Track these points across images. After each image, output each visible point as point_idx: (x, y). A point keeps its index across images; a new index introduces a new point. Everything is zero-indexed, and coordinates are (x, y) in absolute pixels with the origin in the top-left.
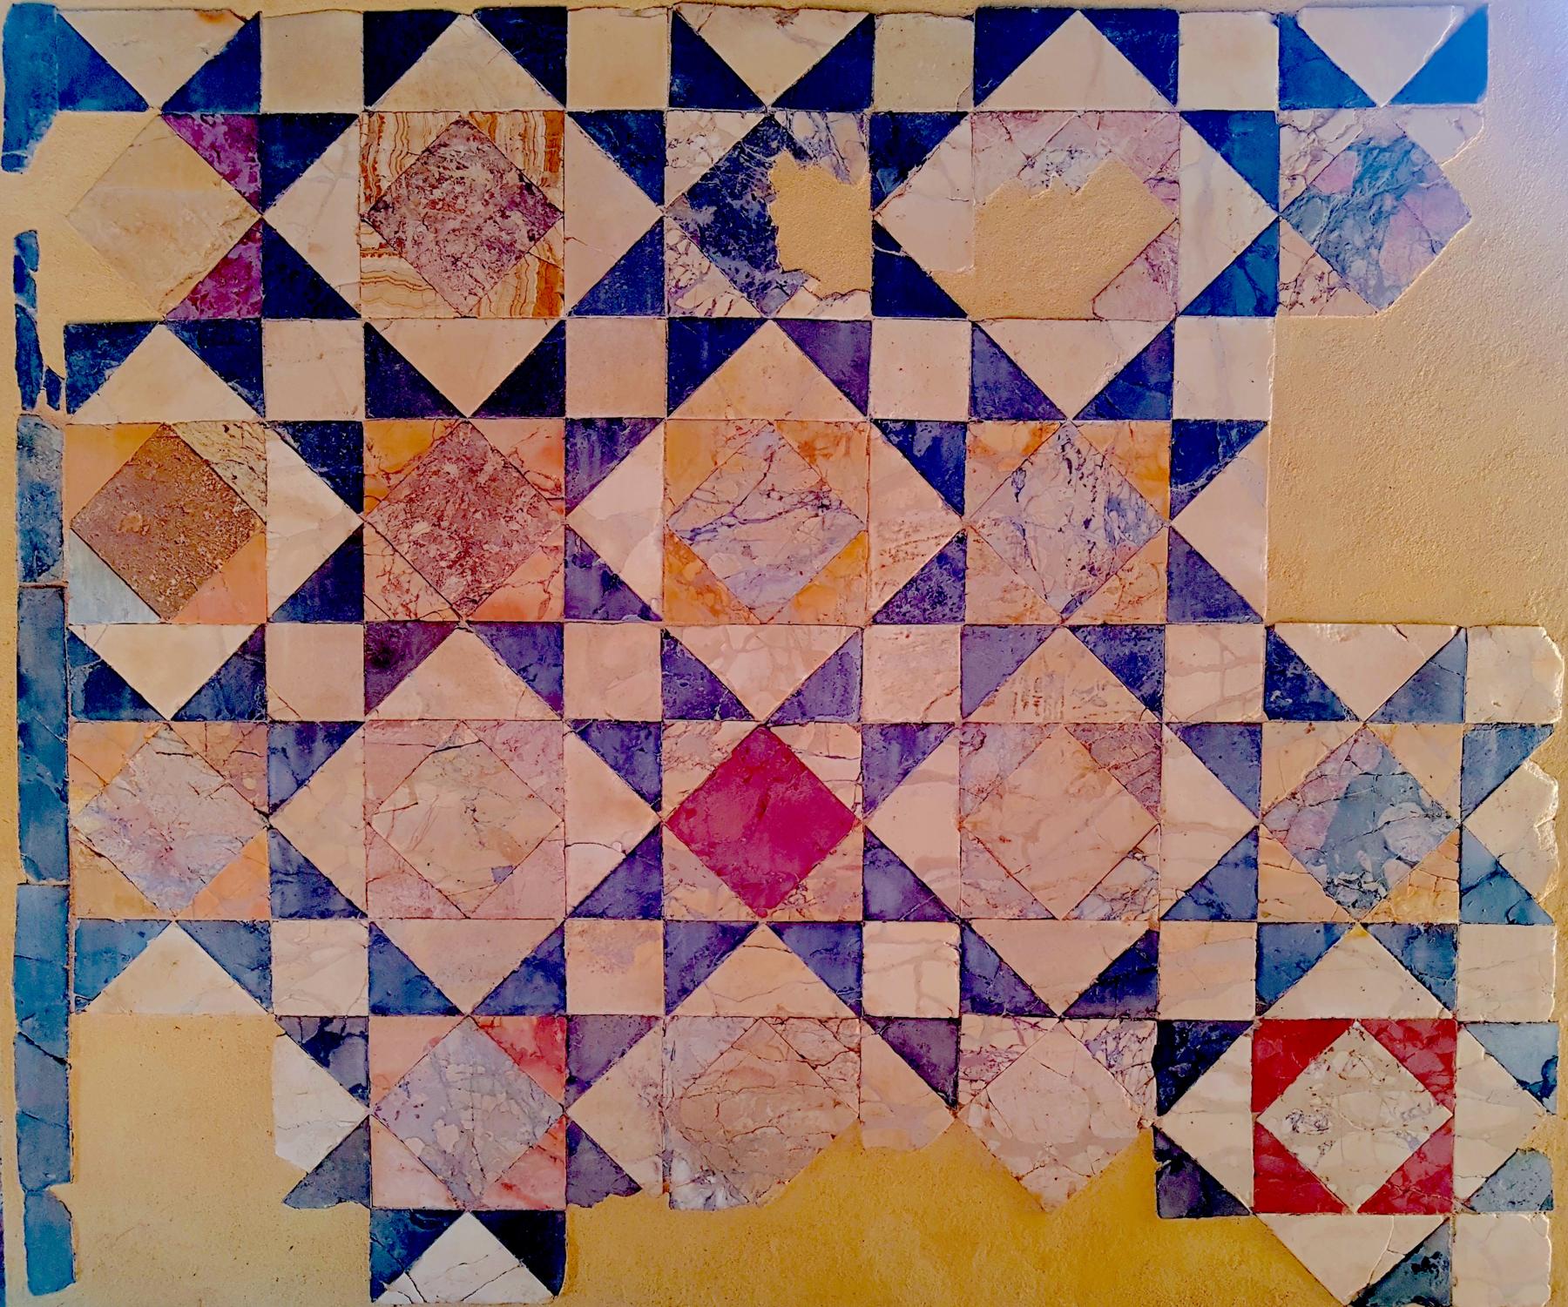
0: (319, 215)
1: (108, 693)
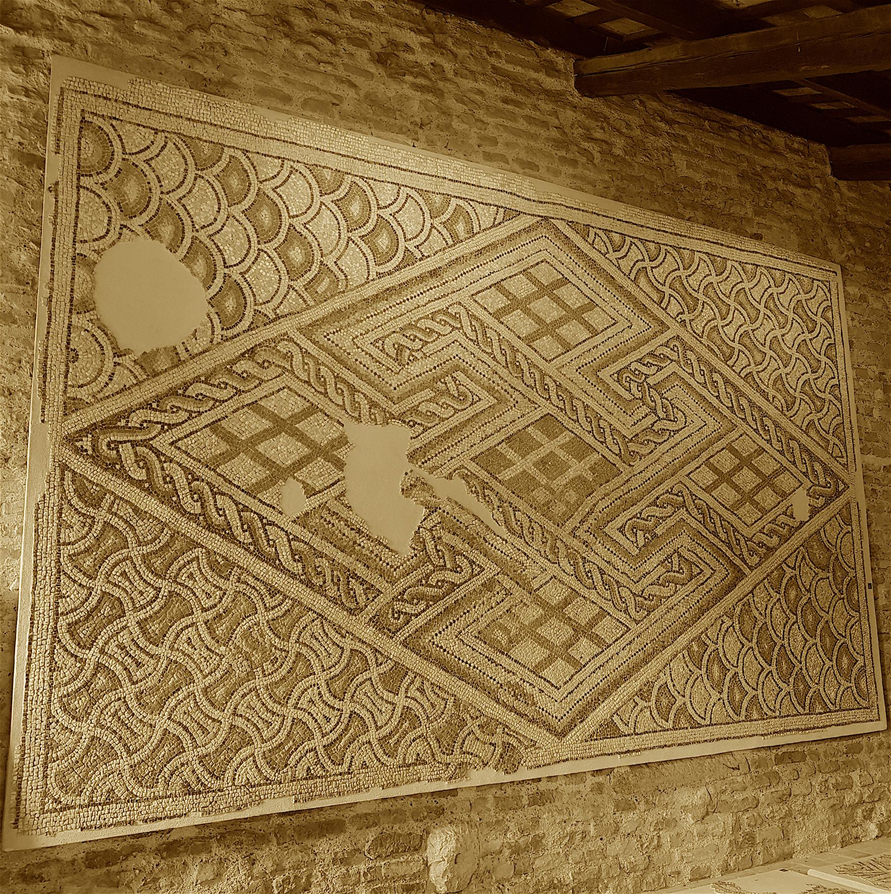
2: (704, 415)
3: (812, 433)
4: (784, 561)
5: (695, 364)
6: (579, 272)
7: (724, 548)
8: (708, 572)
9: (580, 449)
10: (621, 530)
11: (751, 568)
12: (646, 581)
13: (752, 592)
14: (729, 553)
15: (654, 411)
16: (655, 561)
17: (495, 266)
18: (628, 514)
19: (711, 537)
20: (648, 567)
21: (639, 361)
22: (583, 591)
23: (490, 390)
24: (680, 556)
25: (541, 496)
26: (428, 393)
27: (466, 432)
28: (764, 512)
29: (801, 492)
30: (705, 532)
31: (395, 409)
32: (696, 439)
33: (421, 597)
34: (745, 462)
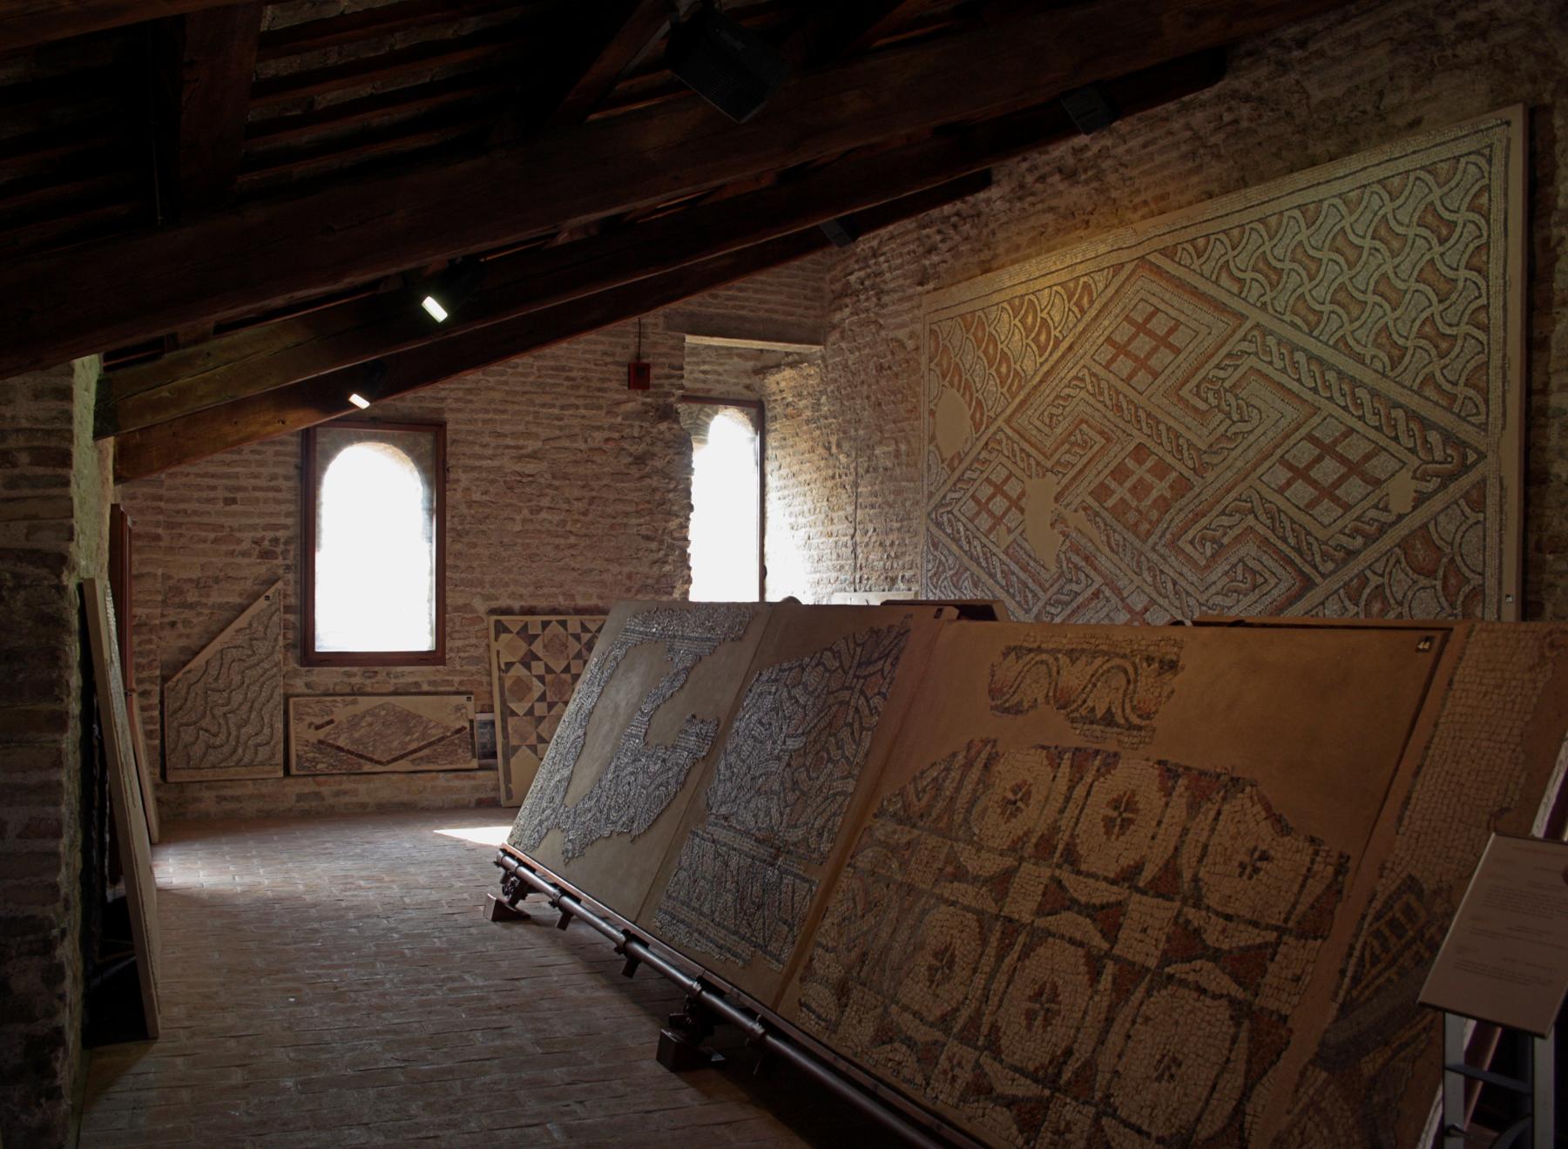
0: (537, 647)
1: (513, 713)
2: (1279, 405)
3: (1429, 392)
4: (1369, 567)
5: (1274, 349)
6: (1167, 296)
7: (1293, 555)
8: (1273, 581)
9: (1161, 470)
10: (1192, 542)
11: (1323, 576)
12: (1213, 590)
13: (1323, 603)
14: (1298, 560)
15: (1228, 415)
16: (1220, 571)
17: (1106, 323)
18: (1198, 526)
19: (1279, 544)
20: (1213, 578)
21: (1217, 367)
22: (1160, 600)
23: (1102, 433)
24: (1245, 565)
25: (1132, 517)
26: (1067, 446)
27: (1086, 472)
28: (1347, 507)
29: (1405, 475)
30: (1273, 539)
31: (1049, 464)
32: (1270, 434)
33: (1059, 602)
34: (1326, 450)
